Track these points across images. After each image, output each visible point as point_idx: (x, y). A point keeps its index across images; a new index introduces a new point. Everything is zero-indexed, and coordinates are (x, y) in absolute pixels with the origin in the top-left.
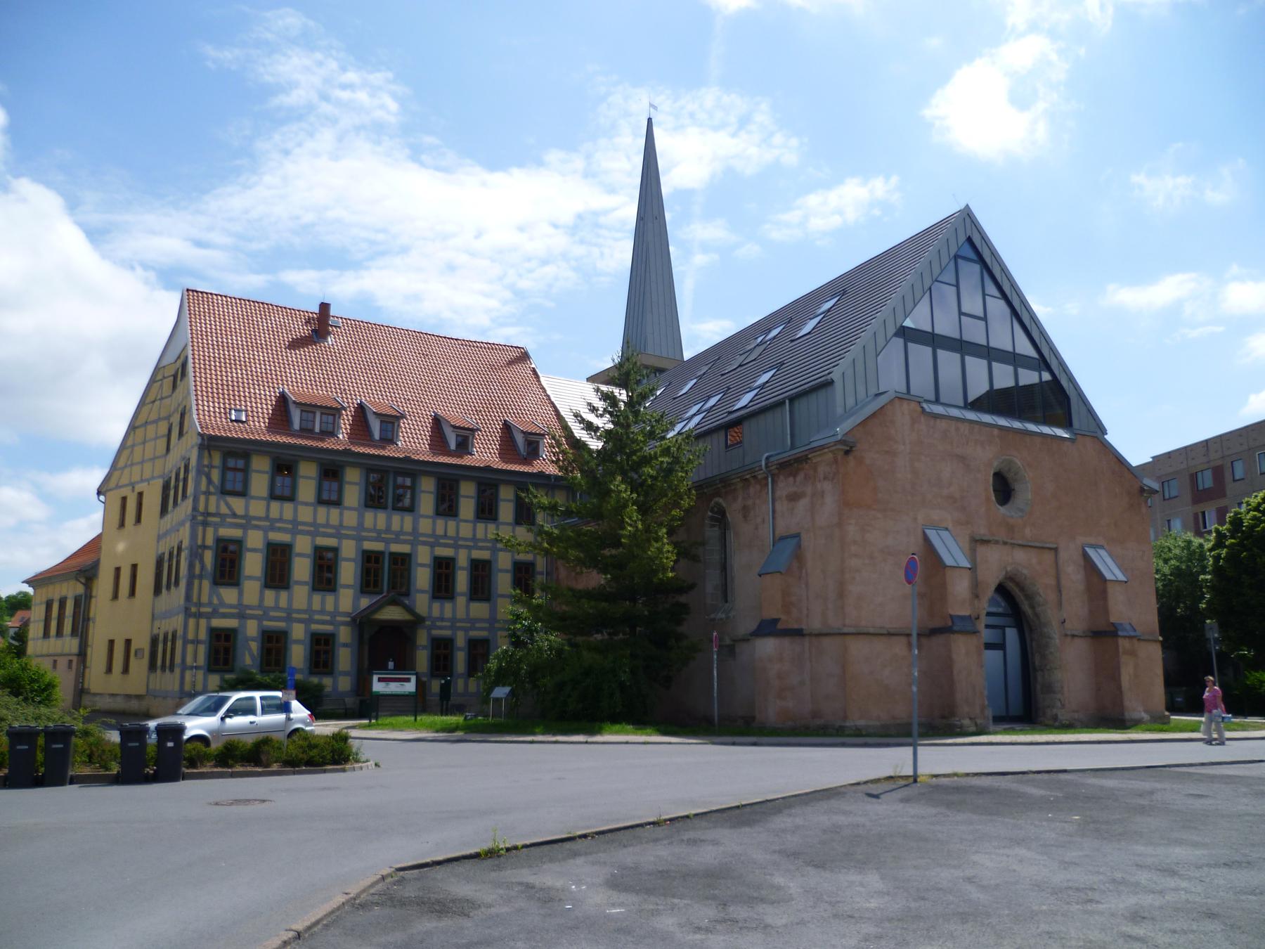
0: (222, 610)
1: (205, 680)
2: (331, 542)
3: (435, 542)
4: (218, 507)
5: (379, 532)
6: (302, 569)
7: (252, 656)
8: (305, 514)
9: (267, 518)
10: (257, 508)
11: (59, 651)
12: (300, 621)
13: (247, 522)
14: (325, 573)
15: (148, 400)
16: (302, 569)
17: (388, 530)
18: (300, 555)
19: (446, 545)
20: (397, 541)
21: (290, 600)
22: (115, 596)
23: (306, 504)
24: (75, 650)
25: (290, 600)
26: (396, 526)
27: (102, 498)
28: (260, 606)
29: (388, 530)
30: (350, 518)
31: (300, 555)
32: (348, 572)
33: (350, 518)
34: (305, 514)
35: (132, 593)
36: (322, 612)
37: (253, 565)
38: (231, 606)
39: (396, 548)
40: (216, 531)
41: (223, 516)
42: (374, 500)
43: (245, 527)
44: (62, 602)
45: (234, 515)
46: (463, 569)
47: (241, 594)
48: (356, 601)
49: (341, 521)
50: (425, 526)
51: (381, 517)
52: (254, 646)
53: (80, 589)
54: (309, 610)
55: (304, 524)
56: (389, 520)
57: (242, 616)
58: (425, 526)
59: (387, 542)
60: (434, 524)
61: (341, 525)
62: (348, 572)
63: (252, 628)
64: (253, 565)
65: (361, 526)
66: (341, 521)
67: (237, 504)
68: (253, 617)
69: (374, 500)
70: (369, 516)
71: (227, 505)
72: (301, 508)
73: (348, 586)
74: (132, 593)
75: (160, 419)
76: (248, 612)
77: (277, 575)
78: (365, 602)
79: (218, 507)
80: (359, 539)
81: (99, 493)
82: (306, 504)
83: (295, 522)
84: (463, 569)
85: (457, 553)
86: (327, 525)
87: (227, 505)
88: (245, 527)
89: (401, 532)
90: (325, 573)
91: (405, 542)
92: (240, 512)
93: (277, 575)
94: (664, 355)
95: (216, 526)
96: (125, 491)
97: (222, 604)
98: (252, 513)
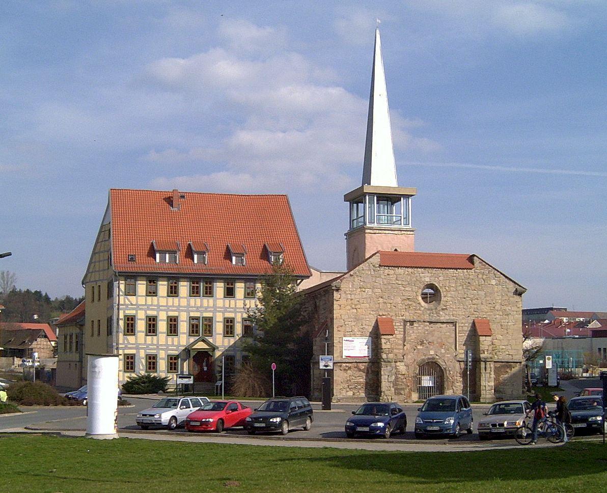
0: (129, 346)
1: (123, 376)
2: (176, 314)
3: (225, 310)
4: (125, 302)
5: (198, 308)
6: (162, 326)
7: (143, 365)
8: (163, 302)
9: (146, 305)
10: (142, 301)
11: (74, 360)
12: (162, 349)
13: (138, 307)
14: (173, 328)
15: (100, 241)
16: (162, 326)
17: (201, 306)
18: (161, 320)
19: (230, 312)
20: (206, 311)
21: (158, 341)
22: (92, 335)
23: (163, 297)
24: (78, 359)
25: (158, 341)
26: (205, 305)
27: (84, 286)
28: (145, 343)
29: (201, 306)
30: (184, 302)
31: (161, 320)
32: (183, 327)
33: (184, 302)
34: (163, 302)
35: (99, 334)
36: (173, 345)
37: (141, 326)
38: (133, 344)
39: (206, 315)
40: (124, 312)
41: (127, 305)
42: (194, 292)
43: (136, 310)
44: (71, 336)
45: (132, 304)
46: (239, 322)
47: (136, 339)
48: (188, 340)
49: (179, 304)
50: (220, 303)
51: (198, 300)
52: (144, 361)
53: (78, 331)
54: (167, 345)
55: (162, 306)
56: (201, 302)
57: (137, 348)
58: (220, 303)
59: (201, 312)
60: (224, 302)
61: (179, 305)
62: (183, 327)
63: (142, 354)
64: (141, 326)
65: (189, 305)
66: (179, 304)
67: (133, 299)
68: (142, 348)
69: (194, 292)
70: (192, 300)
71: (128, 299)
72: (161, 299)
73: (184, 333)
74: (99, 334)
75: (105, 251)
76: (140, 346)
77: (152, 327)
78: (192, 340)
79: (125, 302)
80: (188, 312)
81: (83, 284)
82: (163, 297)
83: (158, 306)
84: (239, 322)
85: (236, 315)
86: (173, 306)
87: (128, 299)
88: (136, 310)
89: (208, 307)
90: (173, 328)
91: (210, 311)
92: (134, 303)
93: (152, 327)
94: (229, 274)
95: (124, 310)
96: (94, 284)
97: (129, 343)
98: (139, 303)
